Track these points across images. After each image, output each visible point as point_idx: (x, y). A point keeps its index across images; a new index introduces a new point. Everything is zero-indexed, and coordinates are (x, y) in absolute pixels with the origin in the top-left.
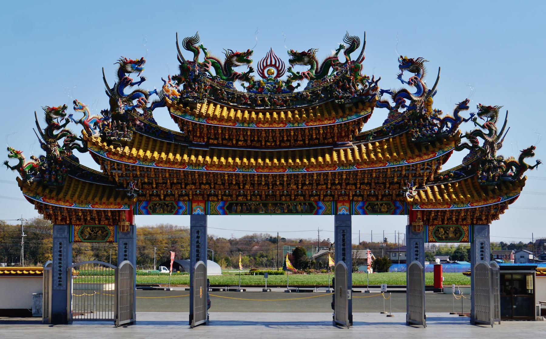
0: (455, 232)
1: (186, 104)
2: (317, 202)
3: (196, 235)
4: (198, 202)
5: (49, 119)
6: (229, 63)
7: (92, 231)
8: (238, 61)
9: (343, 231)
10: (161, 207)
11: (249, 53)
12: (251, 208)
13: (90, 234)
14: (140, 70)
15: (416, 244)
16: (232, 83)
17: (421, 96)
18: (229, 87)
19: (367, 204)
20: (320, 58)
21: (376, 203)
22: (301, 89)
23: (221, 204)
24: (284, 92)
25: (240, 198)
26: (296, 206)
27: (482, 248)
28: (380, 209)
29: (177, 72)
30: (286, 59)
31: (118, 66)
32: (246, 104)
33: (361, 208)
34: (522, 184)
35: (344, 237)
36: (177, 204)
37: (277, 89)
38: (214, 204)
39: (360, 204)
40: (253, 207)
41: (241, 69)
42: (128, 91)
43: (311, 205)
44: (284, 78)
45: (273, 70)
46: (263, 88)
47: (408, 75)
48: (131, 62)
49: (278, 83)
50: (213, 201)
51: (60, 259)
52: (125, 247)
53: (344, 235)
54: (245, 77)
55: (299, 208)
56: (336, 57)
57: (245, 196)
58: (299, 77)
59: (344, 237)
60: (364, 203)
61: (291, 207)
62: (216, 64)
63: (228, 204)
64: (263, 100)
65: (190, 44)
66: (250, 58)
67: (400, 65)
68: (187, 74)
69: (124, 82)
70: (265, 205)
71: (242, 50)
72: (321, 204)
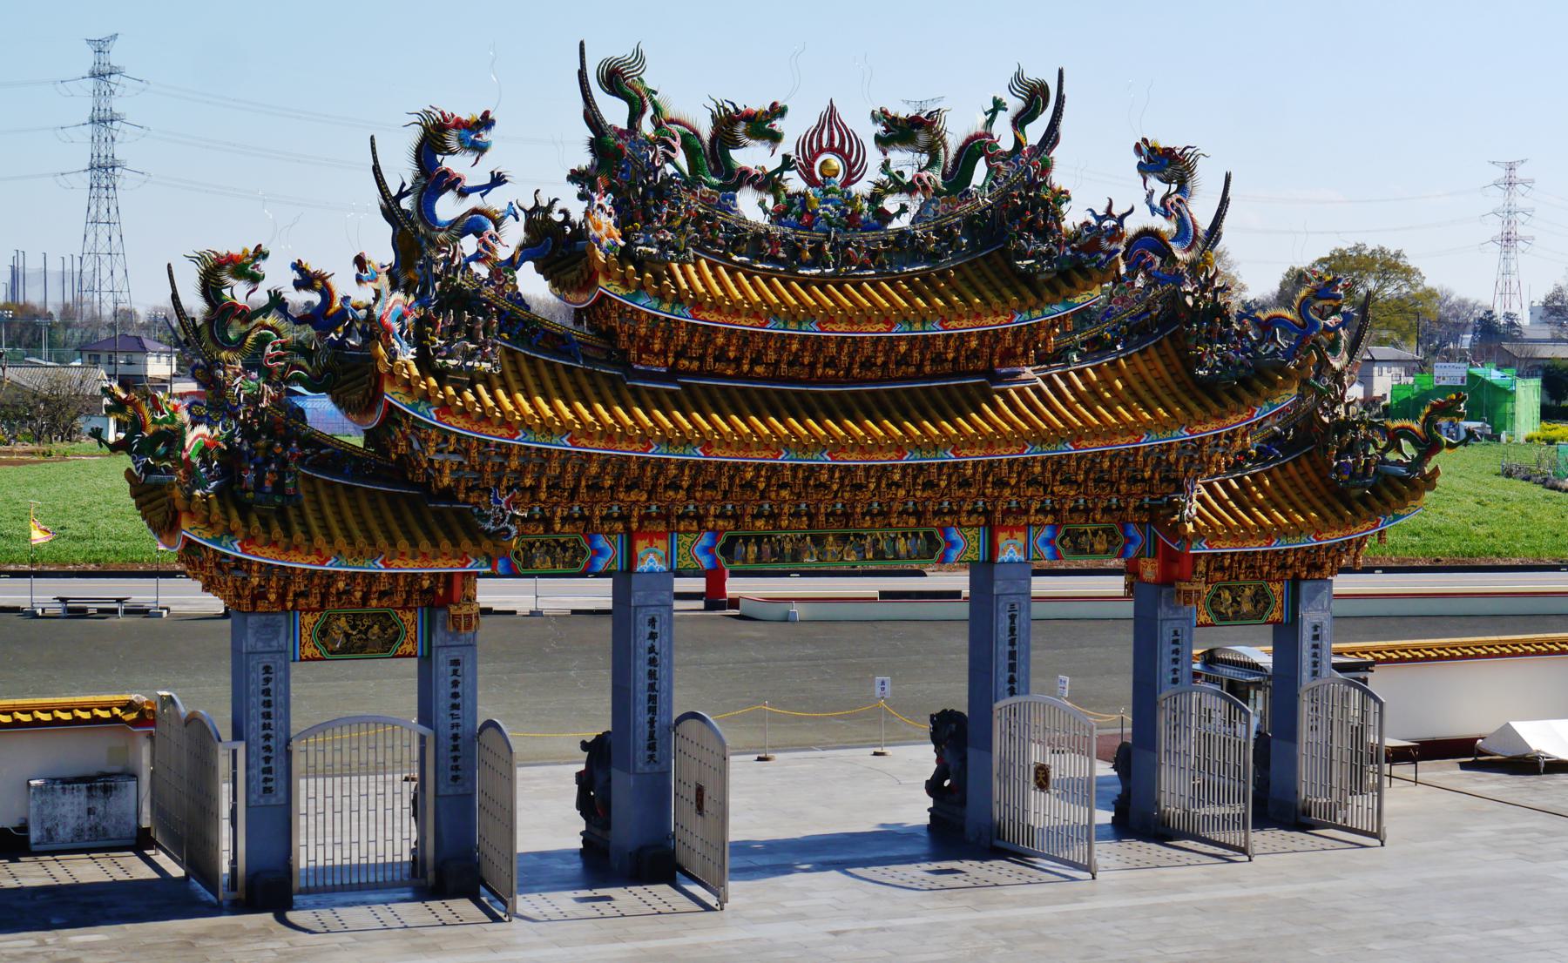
0: (1255, 599)
1: (641, 263)
2: (944, 530)
3: (648, 630)
4: (652, 536)
5: (211, 286)
7: (353, 627)
9: (1012, 606)
10: (547, 552)
11: (778, 111)
12: (782, 550)
13: (347, 635)
14: (480, 149)
15: (1176, 633)
16: (733, 198)
17: (1189, 249)
18: (727, 210)
19: (1062, 533)
20: (955, 133)
21: (1082, 528)
22: (904, 222)
23: (705, 540)
25: (760, 523)
26: (894, 540)
27: (1316, 637)
28: (1092, 545)
29: (584, 160)
30: (867, 132)
31: (414, 135)
32: (773, 259)
33: (1049, 542)
34: (1430, 481)
35: (1013, 622)
36: (591, 541)
37: (848, 217)
38: (687, 540)
39: (1046, 533)
40: (788, 547)
41: (752, 156)
43: (930, 537)
45: (836, 162)
46: (815, 212)
48: (459, 124)
49: (851, 200)
50: (687, 532)
51: (267, 716)
52: (455, 672)
53: (1012, 618)
54: (768, 183)
55: (902, 545)
57: (773, 517)
58: (897, 185)
59: (1013, 622)
60: (1055, 528)
61: (883, 545)
62: (690, 141)
63: (723, 540)
65: (614, 79)
66: (779, 125)
67: (1140, 163)
68: (613, 163)
69: (433, 181)
72: (954, 535)
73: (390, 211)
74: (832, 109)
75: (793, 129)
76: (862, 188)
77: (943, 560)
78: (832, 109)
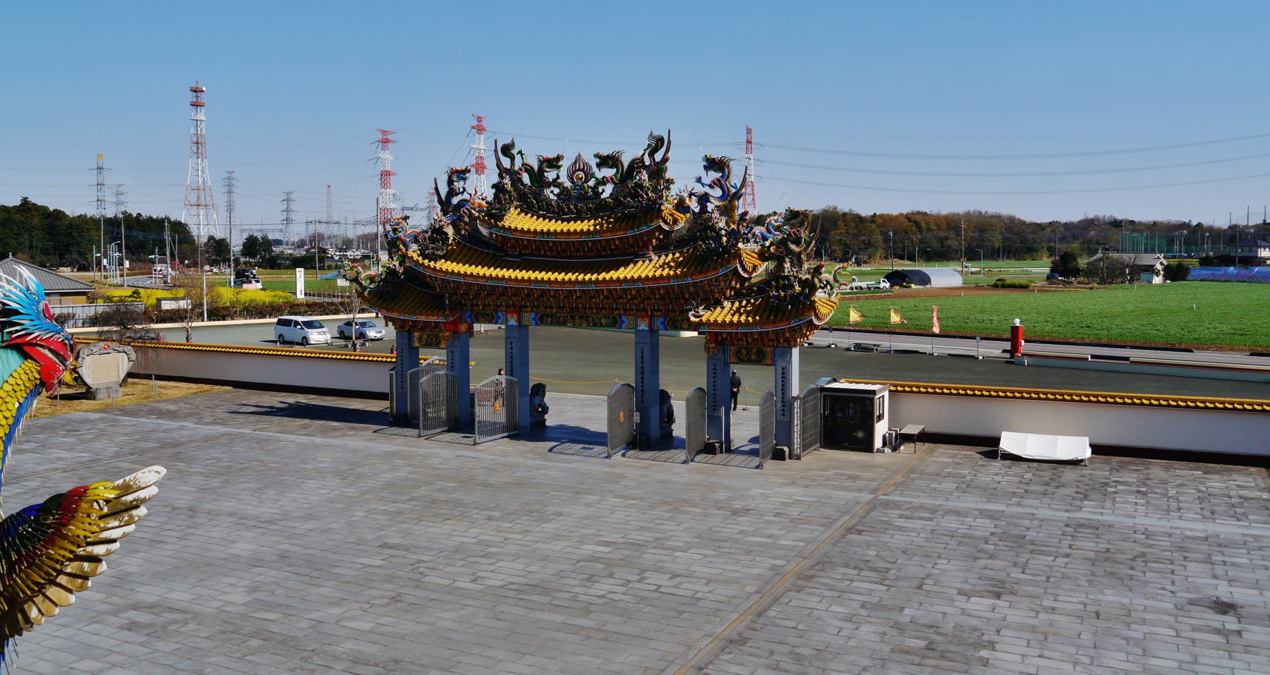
2: (620, 316)
4: (512, 313)
11: (559, 158)
14: (465, 179)
20: (626, 161)
24: (590, 198)
30: (593, 162)
31: (446, 177)
39: (661, 319)
41: (551, 175)
42: (455, 200)
43: (614, 318)
44: (592, 183)
48: (457, 171)
54: (555, 183)
56: (641, 160)
58: (603, 182)
60: (665, 318)
62: (529, 170)
65: (507, 150)
69: (452, 193)
70: (573, 318)
71: (552, 155)
72: (624, 318)
75: (565, 164)
76: (592, 183)
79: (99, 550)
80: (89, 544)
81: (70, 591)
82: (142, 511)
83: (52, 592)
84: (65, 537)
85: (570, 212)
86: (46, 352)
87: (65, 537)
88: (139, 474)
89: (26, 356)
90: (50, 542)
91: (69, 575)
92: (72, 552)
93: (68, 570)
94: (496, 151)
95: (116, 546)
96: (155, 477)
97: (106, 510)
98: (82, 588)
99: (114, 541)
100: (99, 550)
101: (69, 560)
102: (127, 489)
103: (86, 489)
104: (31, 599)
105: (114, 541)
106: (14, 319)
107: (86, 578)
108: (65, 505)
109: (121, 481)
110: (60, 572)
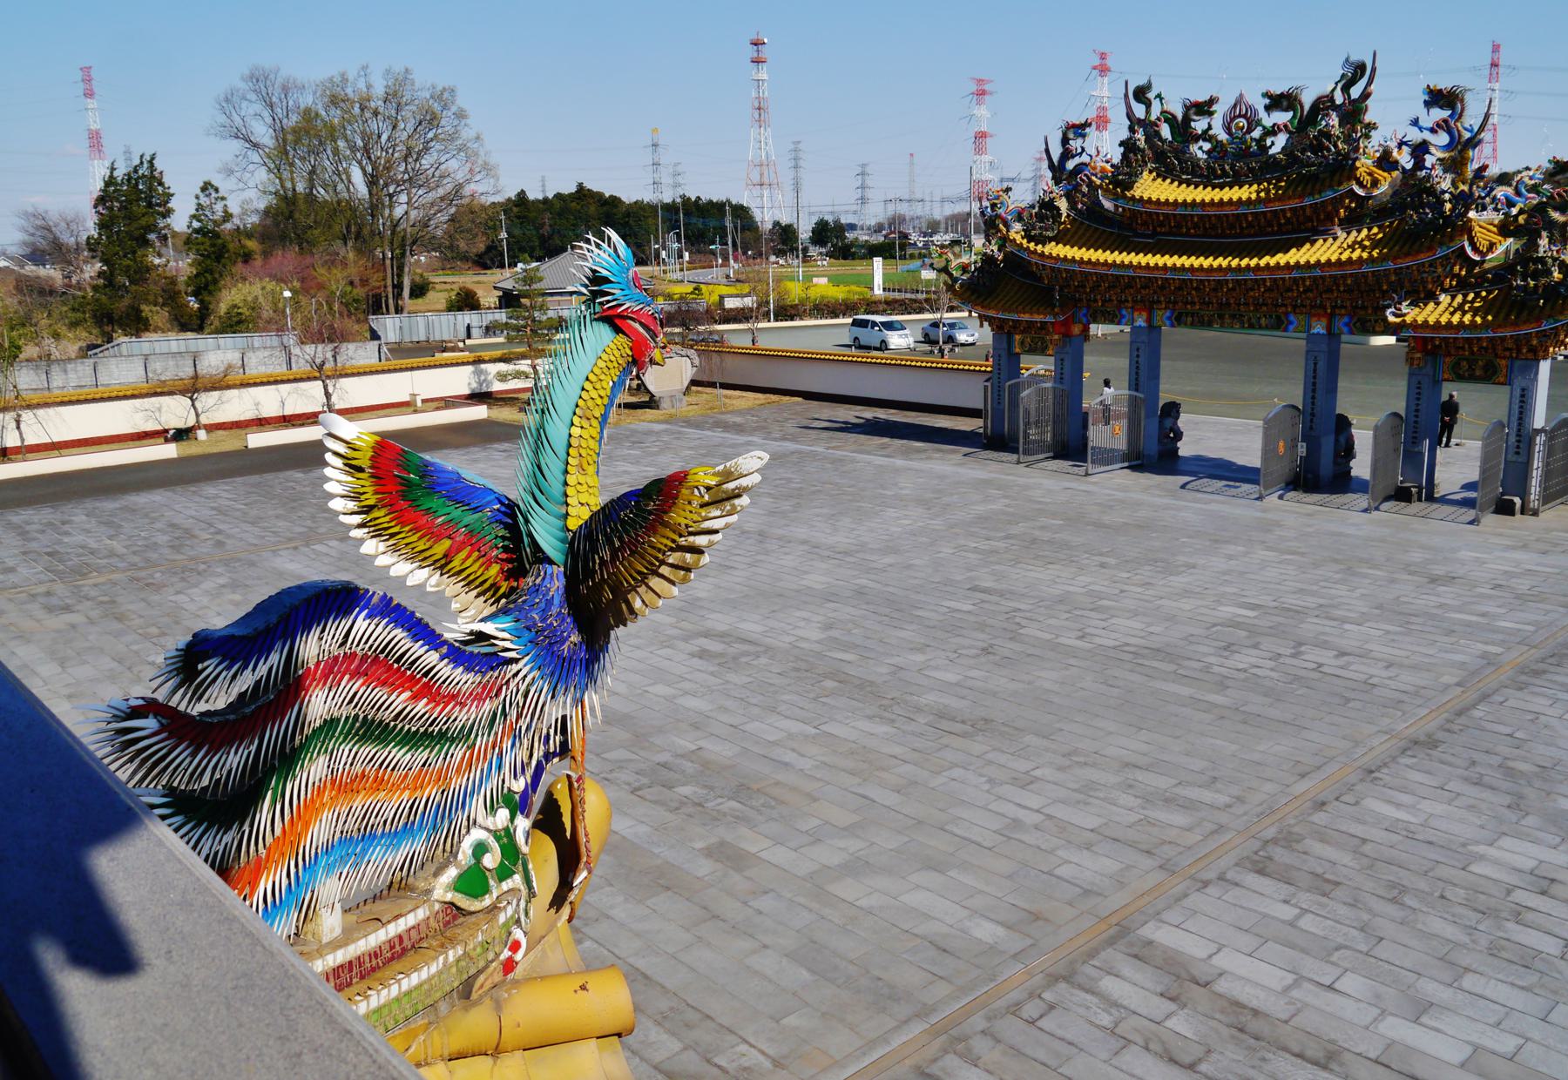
0: (1486, 368)
2: (1287, 314)
4: (1140, 310)
6: (1187, 119)
8: (1197, 114)
11: (1212, 101)
14: (1084, 136)
18: (1184, 153)
20: (1307, 100)
24: (1254, 155)
30: (1260, 104)
31: (1060, 135)
32: (1201, 176)
33: (1346, 324)
39: (1346, 319)
41: (1199, 125)
42: (1070, 165)
43: (1278, 318)
44: (1257, 134)
47: (1439, 114)
48: (1074, 126)
55: (1263, 321)
56: (1331, 98)
58: (1273, 131)
60: (1351, 318)
62: (1170, 118)
64: (1223, 170)
65: (1141, 94)
66: (1214, 108)
69: (1067, 155)
70: (1221, 317)
72: (1292, 318)
73: (1051, 166)
74: (1241, 95)
75: (1220, 110)
76: (1257, 134)
77: (1285, 330)
78: (1241, 95)
79: (701, 541)
80: (691, 534)
81: (673, 583)
82: (744, 500)
83: (655, 582)
84: (666, 525)
85: (1225, 174)
86: (637, 326)
87: (666, 525)
88: (740, 460)
89: (618, 330)
90: (652, 529)
91: (672, 566)
92: (674, 541)
93: (671, 561)
94: (1126, 95)
95: (718, 537)
96: (758, 464)
97: (706, 497)
98: (685, 580)
99: (716, 532)
100: (701, 541)
101: (671, 549)
102: (728, 476)
103: (686, 474)
104: (634, 589)
105: (716, 532)
106: (605, 287)
107: (688, 570)
108: (665, 490)
109: (721, 468)
110: (663, 562)
